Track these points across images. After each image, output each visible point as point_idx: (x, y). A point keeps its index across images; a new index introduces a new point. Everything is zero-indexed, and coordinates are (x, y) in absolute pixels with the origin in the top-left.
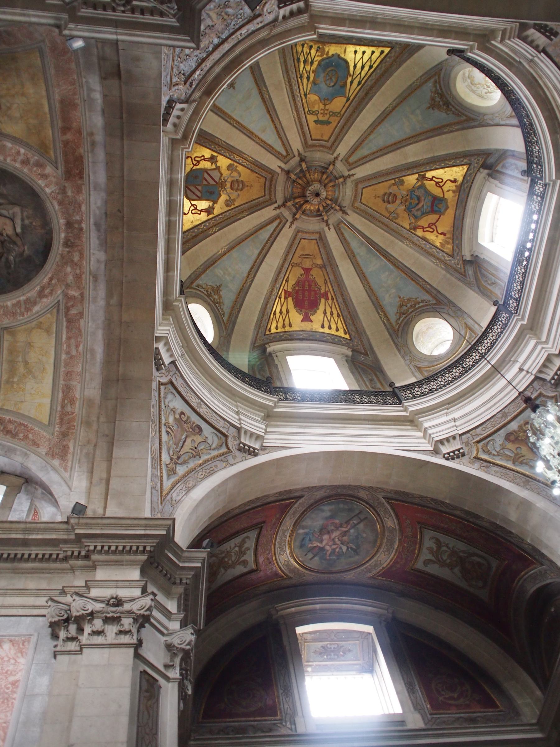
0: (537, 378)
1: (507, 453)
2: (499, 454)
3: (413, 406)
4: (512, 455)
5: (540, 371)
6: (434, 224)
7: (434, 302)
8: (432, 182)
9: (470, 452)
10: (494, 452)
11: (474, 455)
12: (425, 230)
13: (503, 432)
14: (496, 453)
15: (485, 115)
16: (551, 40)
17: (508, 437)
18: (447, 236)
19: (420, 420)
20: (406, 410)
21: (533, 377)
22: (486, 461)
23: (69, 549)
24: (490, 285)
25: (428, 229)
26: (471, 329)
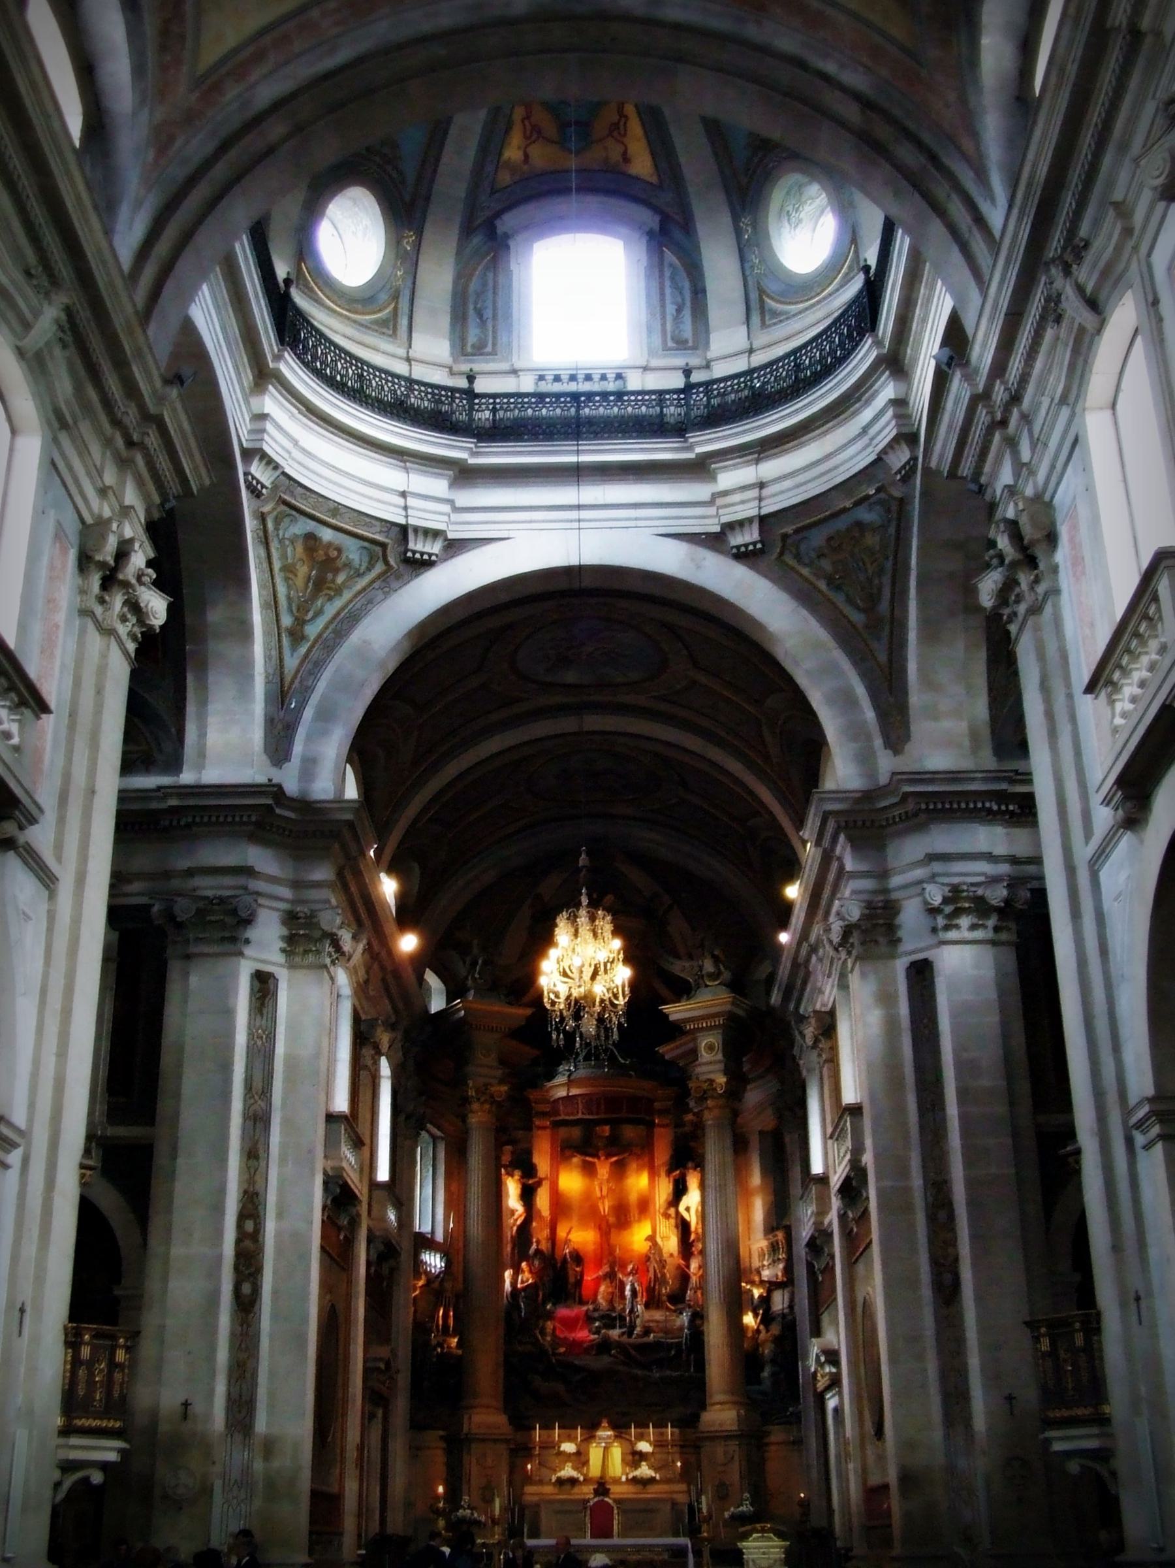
0: (404, 530)
1: (289, 550)
2: (281, 541)
3: (291, 369)
4: (290, 561)
5: (416, 530)
6: (539, 132)
7: (407, 198)
8: (615, 118)
9: (266, 501)
10: (281, 533)
11: (266, 509)
12: (527, 123)
13: (311, 526)
14: (281, 537)
15: (758, 246)
16: (896, 473)
17: (310, 538)
18: (525, 167)
19: (270, 387)
20: (278, 358)
21: (402, 521)
22: (265, 531)
23: (131, 415)
24: (475, 308)
25: (528, 127)
26: (395, 310)
